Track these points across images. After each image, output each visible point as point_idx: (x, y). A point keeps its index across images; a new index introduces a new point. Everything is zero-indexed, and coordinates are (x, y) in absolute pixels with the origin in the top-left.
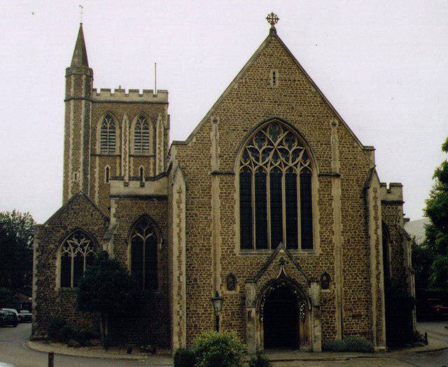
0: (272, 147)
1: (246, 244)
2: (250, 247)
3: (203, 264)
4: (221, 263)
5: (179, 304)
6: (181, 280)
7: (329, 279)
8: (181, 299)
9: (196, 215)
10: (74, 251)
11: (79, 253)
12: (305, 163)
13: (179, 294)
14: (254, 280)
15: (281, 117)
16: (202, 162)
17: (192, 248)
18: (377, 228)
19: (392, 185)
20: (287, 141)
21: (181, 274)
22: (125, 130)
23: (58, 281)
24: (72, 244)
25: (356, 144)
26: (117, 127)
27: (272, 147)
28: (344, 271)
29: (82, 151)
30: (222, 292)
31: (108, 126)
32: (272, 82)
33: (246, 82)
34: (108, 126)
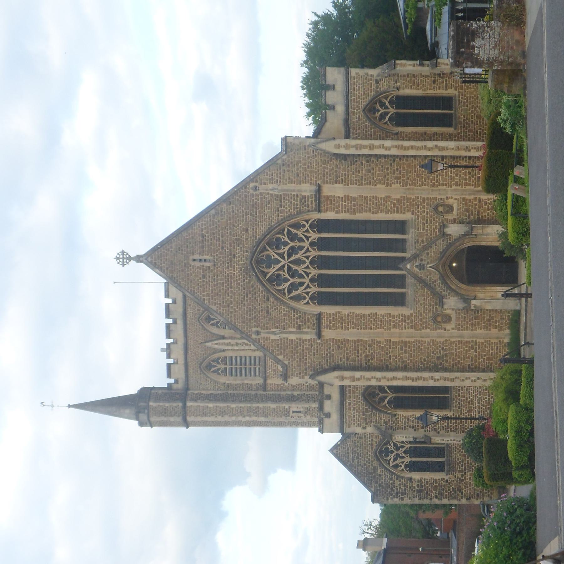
0: (286, 267)
2: (403, 295)
3: (422, 349)
5: (463, 380)
6: (439, 378)
8: (458, 378)
9: (367, 356)
10: (403, 457)
11: (405, 452)
12: (304, 226)
13: (453, 380)
14: (441, 300)
15: (248, 254)
16: (307, 349)
17: (403, 362)
18: (383, 146)
20: (278, 248)
21: (432, 378)
22: (228, 344)
23: (438, 476)
24: (395, 460)
26: (222, 354)
27: (286, 267)
28: (433, 185)
29: (261, 405)
30: (453, 329)
31: (223, 366)
32: (207, 264)
33: (208, 295)
34: (223, 366)
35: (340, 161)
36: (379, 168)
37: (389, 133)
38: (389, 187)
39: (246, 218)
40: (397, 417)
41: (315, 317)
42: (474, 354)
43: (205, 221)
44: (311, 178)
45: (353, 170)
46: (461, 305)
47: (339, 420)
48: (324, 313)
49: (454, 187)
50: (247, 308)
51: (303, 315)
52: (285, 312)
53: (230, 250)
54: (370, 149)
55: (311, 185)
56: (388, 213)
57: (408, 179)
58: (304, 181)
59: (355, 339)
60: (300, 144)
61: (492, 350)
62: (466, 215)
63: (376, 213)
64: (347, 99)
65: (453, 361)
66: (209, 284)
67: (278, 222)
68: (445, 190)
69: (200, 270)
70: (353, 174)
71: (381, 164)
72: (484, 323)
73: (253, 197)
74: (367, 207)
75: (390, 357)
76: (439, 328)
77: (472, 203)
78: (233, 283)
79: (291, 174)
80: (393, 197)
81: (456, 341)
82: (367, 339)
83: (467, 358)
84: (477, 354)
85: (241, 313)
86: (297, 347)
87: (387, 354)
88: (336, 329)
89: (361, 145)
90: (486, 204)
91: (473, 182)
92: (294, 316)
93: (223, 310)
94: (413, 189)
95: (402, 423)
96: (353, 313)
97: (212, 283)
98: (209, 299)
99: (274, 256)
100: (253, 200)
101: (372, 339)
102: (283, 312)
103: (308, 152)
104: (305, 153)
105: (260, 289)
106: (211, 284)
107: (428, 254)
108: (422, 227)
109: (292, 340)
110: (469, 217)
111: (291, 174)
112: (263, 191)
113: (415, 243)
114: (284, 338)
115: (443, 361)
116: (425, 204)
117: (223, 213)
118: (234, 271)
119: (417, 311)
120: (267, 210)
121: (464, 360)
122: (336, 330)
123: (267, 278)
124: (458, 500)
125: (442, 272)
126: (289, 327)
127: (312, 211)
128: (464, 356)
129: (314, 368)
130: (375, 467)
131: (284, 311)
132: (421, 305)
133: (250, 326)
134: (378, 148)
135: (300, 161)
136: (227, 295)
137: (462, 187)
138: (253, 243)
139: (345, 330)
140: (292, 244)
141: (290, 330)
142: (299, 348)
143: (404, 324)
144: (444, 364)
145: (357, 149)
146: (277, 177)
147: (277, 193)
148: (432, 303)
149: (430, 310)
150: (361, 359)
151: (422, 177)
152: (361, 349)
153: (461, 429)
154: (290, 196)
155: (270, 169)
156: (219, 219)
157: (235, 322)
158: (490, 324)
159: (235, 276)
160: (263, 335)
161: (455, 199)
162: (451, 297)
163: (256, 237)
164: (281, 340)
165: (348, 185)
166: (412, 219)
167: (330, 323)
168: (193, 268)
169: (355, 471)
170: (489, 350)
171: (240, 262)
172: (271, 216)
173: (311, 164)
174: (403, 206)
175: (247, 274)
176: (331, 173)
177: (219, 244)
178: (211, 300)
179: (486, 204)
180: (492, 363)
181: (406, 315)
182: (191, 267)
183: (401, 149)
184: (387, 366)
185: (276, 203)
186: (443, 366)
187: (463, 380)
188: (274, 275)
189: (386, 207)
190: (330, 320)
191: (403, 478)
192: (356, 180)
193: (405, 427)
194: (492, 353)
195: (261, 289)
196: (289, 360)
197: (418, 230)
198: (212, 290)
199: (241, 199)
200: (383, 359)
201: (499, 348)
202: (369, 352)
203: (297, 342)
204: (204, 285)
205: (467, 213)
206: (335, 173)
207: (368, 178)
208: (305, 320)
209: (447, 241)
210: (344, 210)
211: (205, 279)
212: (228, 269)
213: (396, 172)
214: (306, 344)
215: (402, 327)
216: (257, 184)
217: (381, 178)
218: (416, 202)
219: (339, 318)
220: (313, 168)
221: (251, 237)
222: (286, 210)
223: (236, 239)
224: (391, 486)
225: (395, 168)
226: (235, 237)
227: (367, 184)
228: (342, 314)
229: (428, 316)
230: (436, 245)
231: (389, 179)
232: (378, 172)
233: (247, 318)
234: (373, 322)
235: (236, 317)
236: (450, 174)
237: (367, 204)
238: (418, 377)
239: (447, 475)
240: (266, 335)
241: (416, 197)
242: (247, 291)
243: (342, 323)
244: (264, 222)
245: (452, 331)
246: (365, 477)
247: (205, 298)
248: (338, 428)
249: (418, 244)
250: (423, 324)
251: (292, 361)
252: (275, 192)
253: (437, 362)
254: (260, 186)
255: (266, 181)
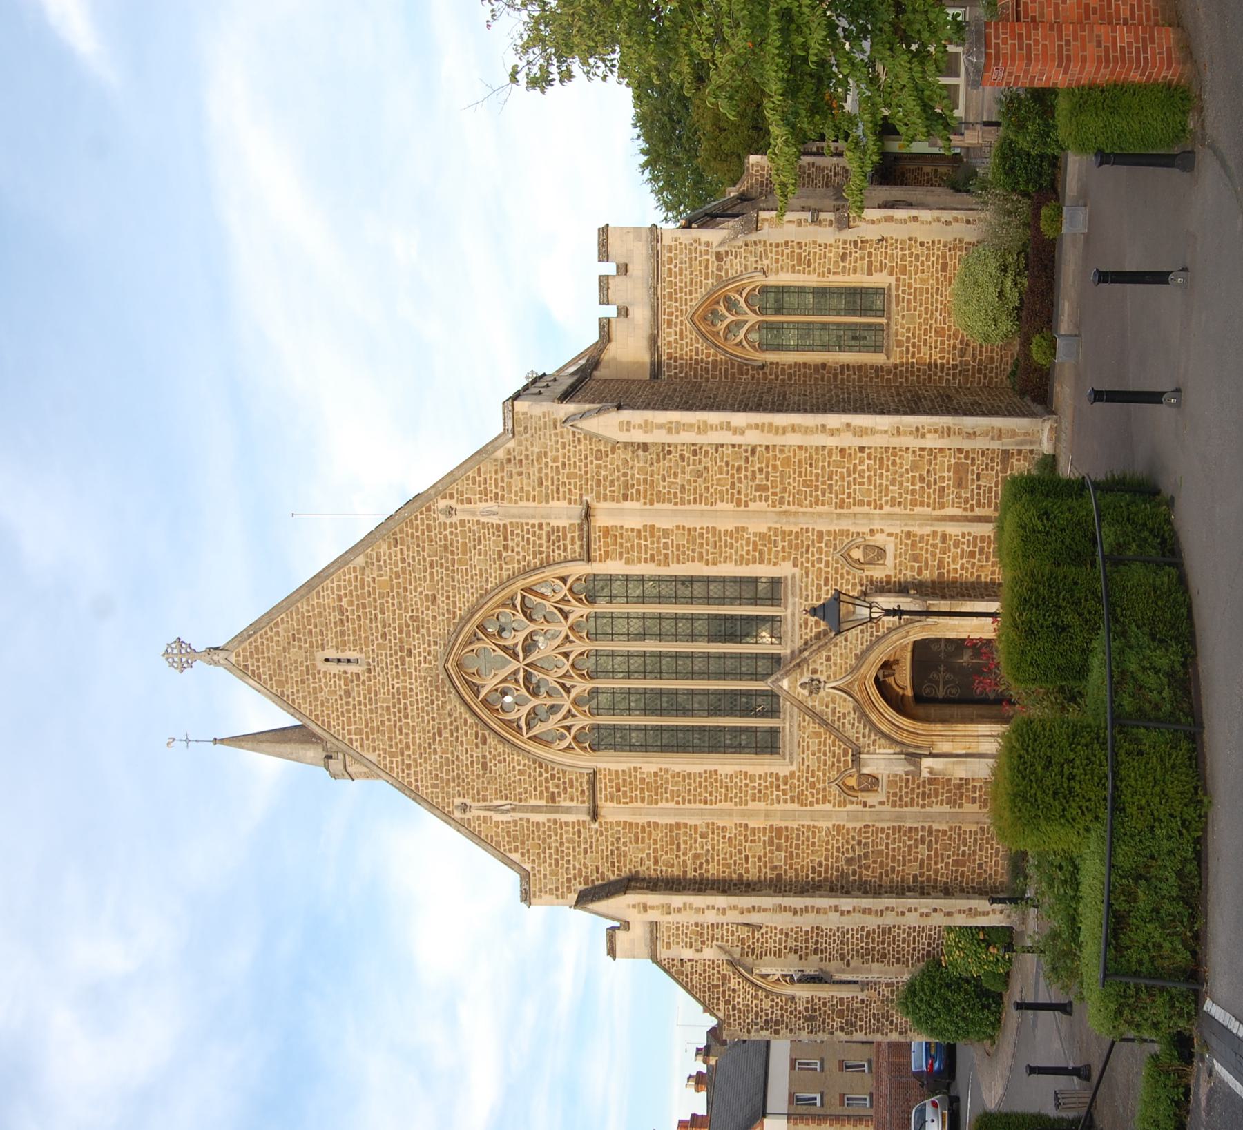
1: (768, 744)
2: (774, 732)
3: (814, 844)
4: (812, 804)
5: (903, 914)
6: (851, 909)
7: (868, 548)
8: (893, 909)
9: (696, 856)
15: (440, 650)
17: (774, 868)
19: (604, 255)
21: (836, 909)
25: (500, 454)
30: (882, 803)
33: (360, 732)
35: (633, 452)
36: (720, 467)
37: (747, 365)
38: (742, 508)
39: (432, 573)
40: (763, 931)
41: (586, 777)
42: (927, 853)
43: (345, 580)
44: (570, 490)
45: (662, 472)
46: (901, 768)
47: (648, 936)
48: (605, 769)
49: (887, 509)
50: (441, 757)
51: (558, 773)
52: (521, 767)
53: (401, 640)
54: (699, 433)
55: (570, 503)
56: (741, 564)
57: (784, 490)
58: (555, 495)
59: (673, 823)
60: (544, 417)
61: (965, 846)
62: (912, 567)
63: (715, 564)
64: (655, 294)
65: (881, 867)
66: (360, 709)
67: (502, 583)
68: (868, 514)
69: (340, 680)
70: (664, 481)
71: (725, 459)
72: (949, 791)
73: (445, 530)
74: (693, 551)
75: (747, 858)
76: (852, 803)
77: (927, 544)
78: (410, 708)
79: (525, 481)
80: (751, 530)
81: (889, 828)
82: (698, 822)
83: (910, 861)
84: (932, 853)
85: (429, 768)
86: (550, 837)
87: (740, 852)
88: (631, 802)
89: (677, 423)
90: (956, 546)
91: (929, 497)
92: (541, 774)
93: (391, 762)
94: (796, 513)
95: (775, 942)
96: (666, 771)
97: (366, 706)
98: (362, 739)
99: (494, 651)
100: (446, 537)
101: (708, 824)
102: (517, 768)
103: (562, 432)
104: (556, 435)
105: (466, 721)
106: (363, 708)
107: (828, 659)
108: (815, 593)
109: (538, 823)
110: (919, 573)
111: (525, 481)
112: (466, 518)
113: (801, 626)
114: (521, 819)
115: (860, 867)
116: (823, 545)
117: (382, 563)
118: (411, 684)
119: (805, 767)
120: (477, 557)
121: (904, 865)
122: (630, 805)
123: (481, 697)
124: (882, 1034)
125: (859, 697)
126: (531, 797)
127: (573, 560)
128: (904, 857)
129: (586, 878)
130: (724, 977)
131: (519, 765)
132: (814, 754)
133: (448, 793)
134: (717, 430)
135: (546, 453)
136: (398, 732)
137: (905, 509)
138: (449, 625)
139: (650, 803)
140: (532, 627)
141: (533, 802)
142: (553, 838)
143: (775, 793)
144: (861, 873)
145: (669, 430)
146: (496, 488)
147: (498, 522)
148: (837, 751)
149: (833, 764)
150: (684, 861)
151: (817, 487)
152: (685, 843)
153: (893, 955)
154: (525, 528)
155: (479, 469)
156: (375, 576)
157: (417, 787)
158: (961, 795)
159: (414, 693)
160: (475, 813)
161: (890, 535)
162: (879, 748)
163: (454, 613)
164: (515, 822)
165: (652, 504)
166: (793, 576)
167: (618, 790)
168: (325, 676)
169: (687, 982)
170: (959, 845)
171: (423, 665)
172: (486, 570)
173: (569, 460)
174: (774, 549)
175: (438, 691)
176: (615, 477)
177: (377, 627)
178: (365, 742)
179: (956, 546)
180: (963, 872)
181: (781, 774)
182: (321, 675)
183: (768, 432)
184: (741, 875)
185: (494, 541)
186: (860, 877)
187: (903, 914)
188: (496, 690)
189: (736, 552)
190: (618, 784)
191: (778, 995)
192: (669, 493)
193: (780, 950)
194: (964, 851)
195: (469, 721)
196: (534, 860)
197: (806, 600)
198: (366, 721)
199: (419, 534)
200: (732, 862)
201: (979, 842)
202: (702, 848)
203: (550, 827)
204: (348, 711)
205: (916, 565)
206: (622, 479)
207: (695, 489)
208: (564, 783)
209: (872, 632)
210: (643, 556)
211: (350, 700)
212: (398, 677)
213: (758, 476)
214: (567, 832)
215: (772, 800)
216: (453, 503)
217: (724, 489)
218: (802, 541)
219: (636, 781)
220: (575, 467)
221: (444, 615)
222: (517, 557)
223: (411, 617)
224: (755, 1009)
225: (756, 469)
226: (410, 614)
227: (695, 501)
228: (643, 773)
229: (829, 778)
230: (846, 640)
231: (743, 491)
232: (718, 476)
233: (442, 778)
234: (709, 789)
235: (420, 776)
236: (878, 481)
237: (694, 543)
238: (806, 907)
239: (862, 991)
240: (482, 813)
241: (802, 529)
242: (440, 724)
243: (642, 789)
244: (470, 583)
245: (879, 808)
246: (705, 992)
247: (354, 737)
248: (646, 950)
249: (806, 628)
250: (818, 793)
251: (539, 865)
252: (494, 520)
253: (848, 869)
254: (459, 507)
255: (472, 497)
